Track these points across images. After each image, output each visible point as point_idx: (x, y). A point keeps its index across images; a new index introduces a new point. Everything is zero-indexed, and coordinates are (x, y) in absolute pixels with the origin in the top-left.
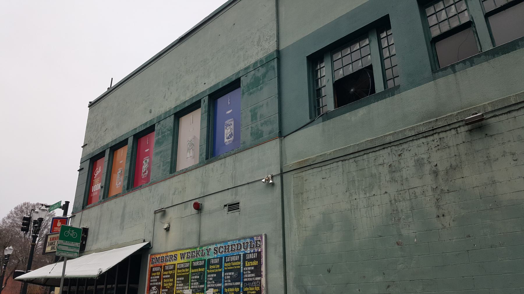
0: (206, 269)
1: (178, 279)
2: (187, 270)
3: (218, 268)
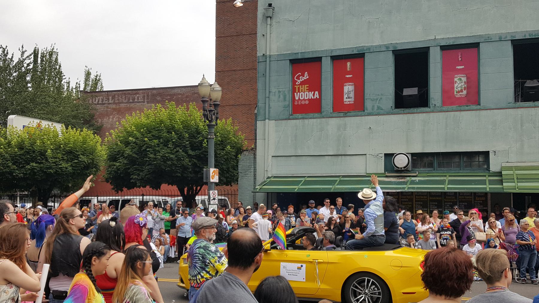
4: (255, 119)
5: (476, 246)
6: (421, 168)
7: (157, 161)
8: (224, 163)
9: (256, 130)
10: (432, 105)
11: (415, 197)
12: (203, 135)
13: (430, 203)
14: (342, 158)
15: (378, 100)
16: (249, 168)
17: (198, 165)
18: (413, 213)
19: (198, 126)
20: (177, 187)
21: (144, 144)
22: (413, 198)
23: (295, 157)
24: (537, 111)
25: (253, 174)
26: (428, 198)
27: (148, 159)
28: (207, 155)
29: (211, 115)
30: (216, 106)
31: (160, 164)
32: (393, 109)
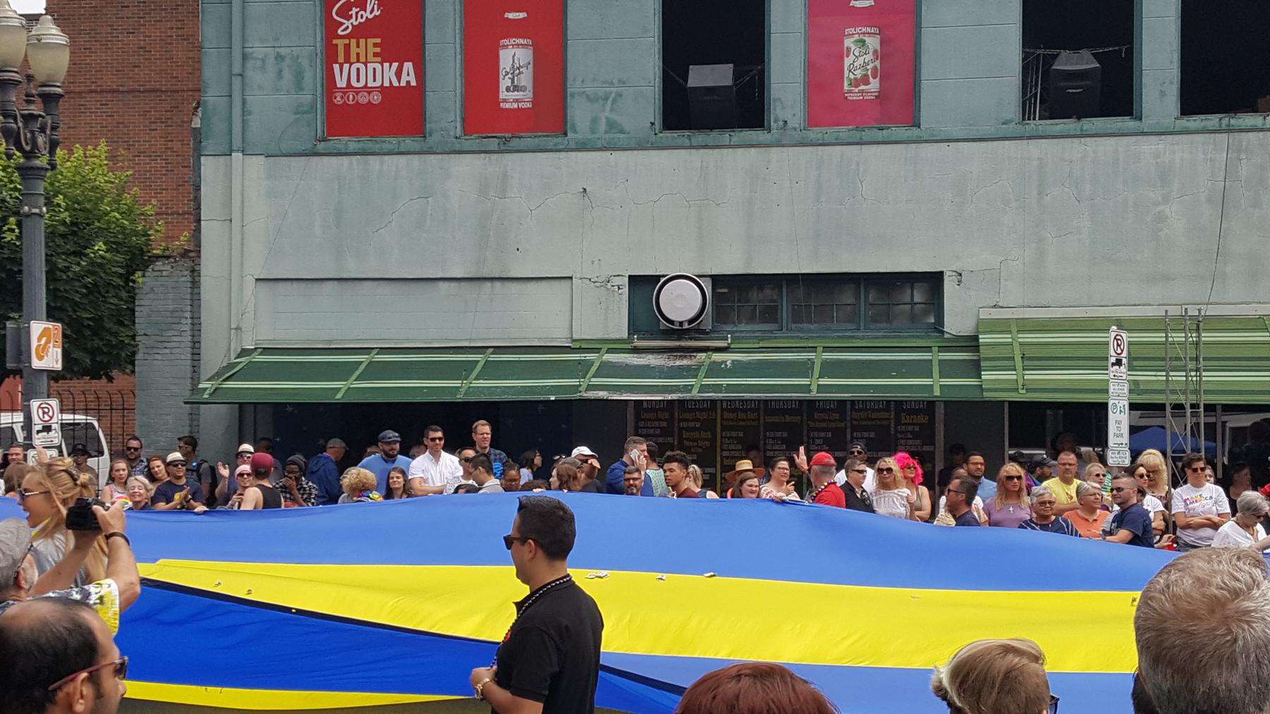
0: (804, 418)
2: (751, 415)
3: (835, 420)
4: (194, 150)
6: (740, 322)
8: (85, 301)
9: (198, 188)
11: (722, 416)
14: (492, 286)
15: (609, 102)
16: (171, 320)
22: (715, 419)
23: (335, 283)
24: (1088, 148)
25: (189, 338)
26: (762, 418)
28: (20, 272)
29: (32, 132)
30: (49, 100)
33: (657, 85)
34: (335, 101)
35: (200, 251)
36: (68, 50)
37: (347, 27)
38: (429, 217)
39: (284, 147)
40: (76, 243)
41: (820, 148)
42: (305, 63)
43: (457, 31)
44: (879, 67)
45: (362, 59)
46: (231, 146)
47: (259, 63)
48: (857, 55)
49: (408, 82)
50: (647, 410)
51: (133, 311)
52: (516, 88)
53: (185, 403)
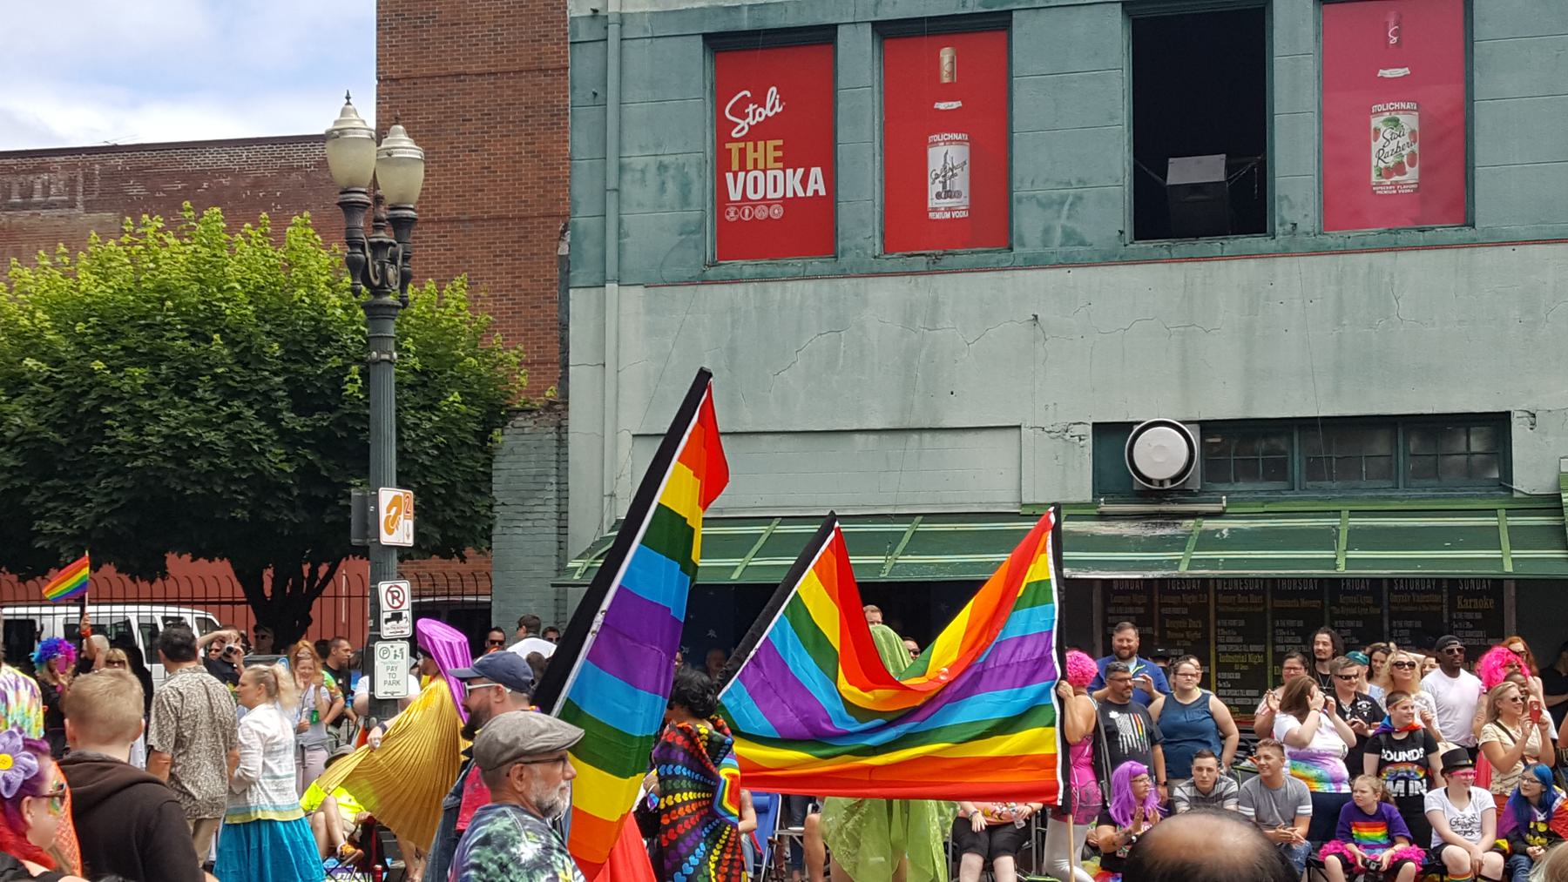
0: (1327, 602)
1: (1225, 623)
2: (1254, 599)
3: (1367, 606)
5: (1473, 795)
6: (1237, 480)
7: (145, 456)
8: (435, 463)
9: (565, 327)
10: (1281, 225)
11: (1216, 600)
12: (344, 347)
13: (1273, 620)
14: (921, 440)
15: (1067, 206)
16: (533, 486)
17: (324, 473)
18: (1209, 665)
19: (322, 312)
20: (232, 562)
21: (91, 387)
25: (554, 508)
27: (110, 446)
31: (159, 468)
32: (1127, 242)
33: (1126, 184)
34: (728, 217)
35: (567, 403)
36: (422, 167)
37: (743, 128)
38: (842, 354)
39: (667, 274)
40: (425, 395)
41: (1341, 256)
42: (693, 173)
43: (877, 128)
44: (1417, 152)
45: (761, 165)
46: (605, 277)
47: (638, 175)
48: (1389, 138)
49: (816, 192)
50: (1120, 593)
51: (489, 477)
52: (949, 194)
53: (553, 585)
